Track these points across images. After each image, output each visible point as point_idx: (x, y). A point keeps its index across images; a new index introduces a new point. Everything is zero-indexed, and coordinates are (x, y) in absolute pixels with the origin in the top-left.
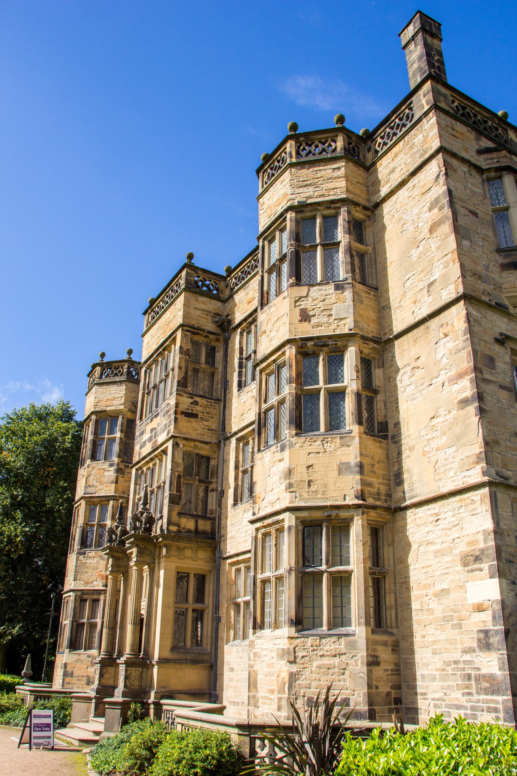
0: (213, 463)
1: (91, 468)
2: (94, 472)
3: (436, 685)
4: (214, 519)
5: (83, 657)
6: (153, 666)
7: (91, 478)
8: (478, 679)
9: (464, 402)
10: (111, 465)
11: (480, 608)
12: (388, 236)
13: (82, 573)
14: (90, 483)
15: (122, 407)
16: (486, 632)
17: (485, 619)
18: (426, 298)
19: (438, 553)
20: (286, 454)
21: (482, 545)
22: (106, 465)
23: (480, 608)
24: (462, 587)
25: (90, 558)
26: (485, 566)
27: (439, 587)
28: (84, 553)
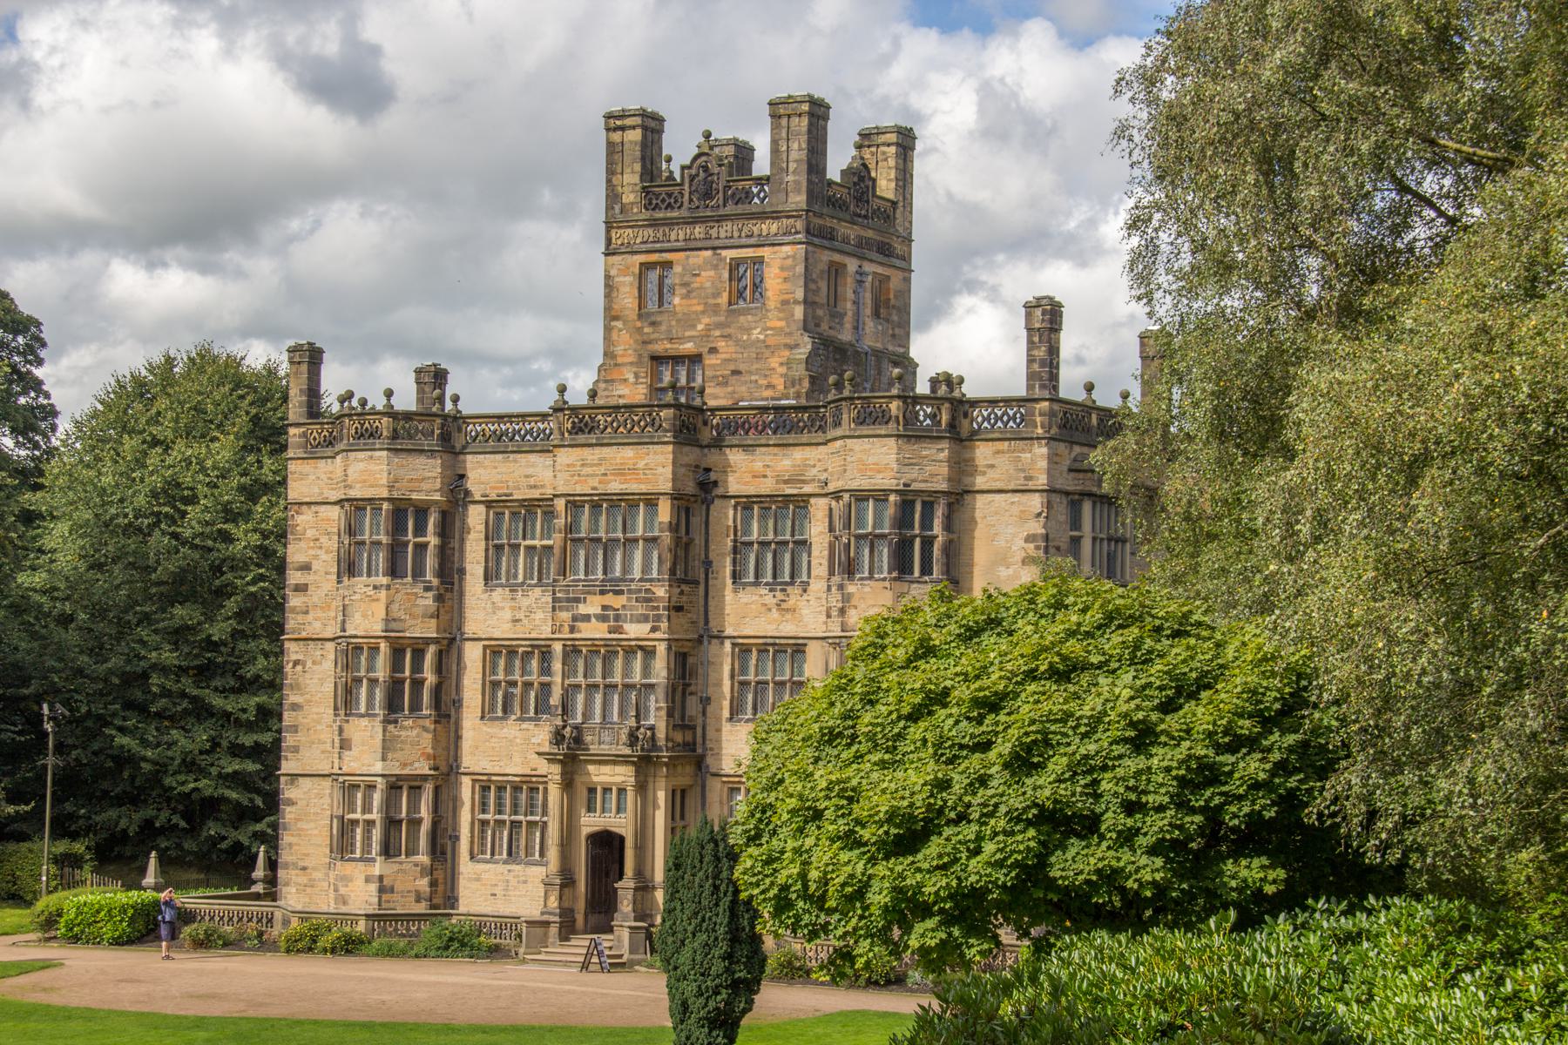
0: (690, 660)
1: (392, 591)
2: (399, 597)
4: (693, 728)
6: (654, 888)
7: (395, 607)
10: (427, 589)
12: (977, 534)
13: (395, 750)
14: (395, 615)
15: (437, 497)
22: (419, 589)
25: (405, 728)
28: (396, 722)
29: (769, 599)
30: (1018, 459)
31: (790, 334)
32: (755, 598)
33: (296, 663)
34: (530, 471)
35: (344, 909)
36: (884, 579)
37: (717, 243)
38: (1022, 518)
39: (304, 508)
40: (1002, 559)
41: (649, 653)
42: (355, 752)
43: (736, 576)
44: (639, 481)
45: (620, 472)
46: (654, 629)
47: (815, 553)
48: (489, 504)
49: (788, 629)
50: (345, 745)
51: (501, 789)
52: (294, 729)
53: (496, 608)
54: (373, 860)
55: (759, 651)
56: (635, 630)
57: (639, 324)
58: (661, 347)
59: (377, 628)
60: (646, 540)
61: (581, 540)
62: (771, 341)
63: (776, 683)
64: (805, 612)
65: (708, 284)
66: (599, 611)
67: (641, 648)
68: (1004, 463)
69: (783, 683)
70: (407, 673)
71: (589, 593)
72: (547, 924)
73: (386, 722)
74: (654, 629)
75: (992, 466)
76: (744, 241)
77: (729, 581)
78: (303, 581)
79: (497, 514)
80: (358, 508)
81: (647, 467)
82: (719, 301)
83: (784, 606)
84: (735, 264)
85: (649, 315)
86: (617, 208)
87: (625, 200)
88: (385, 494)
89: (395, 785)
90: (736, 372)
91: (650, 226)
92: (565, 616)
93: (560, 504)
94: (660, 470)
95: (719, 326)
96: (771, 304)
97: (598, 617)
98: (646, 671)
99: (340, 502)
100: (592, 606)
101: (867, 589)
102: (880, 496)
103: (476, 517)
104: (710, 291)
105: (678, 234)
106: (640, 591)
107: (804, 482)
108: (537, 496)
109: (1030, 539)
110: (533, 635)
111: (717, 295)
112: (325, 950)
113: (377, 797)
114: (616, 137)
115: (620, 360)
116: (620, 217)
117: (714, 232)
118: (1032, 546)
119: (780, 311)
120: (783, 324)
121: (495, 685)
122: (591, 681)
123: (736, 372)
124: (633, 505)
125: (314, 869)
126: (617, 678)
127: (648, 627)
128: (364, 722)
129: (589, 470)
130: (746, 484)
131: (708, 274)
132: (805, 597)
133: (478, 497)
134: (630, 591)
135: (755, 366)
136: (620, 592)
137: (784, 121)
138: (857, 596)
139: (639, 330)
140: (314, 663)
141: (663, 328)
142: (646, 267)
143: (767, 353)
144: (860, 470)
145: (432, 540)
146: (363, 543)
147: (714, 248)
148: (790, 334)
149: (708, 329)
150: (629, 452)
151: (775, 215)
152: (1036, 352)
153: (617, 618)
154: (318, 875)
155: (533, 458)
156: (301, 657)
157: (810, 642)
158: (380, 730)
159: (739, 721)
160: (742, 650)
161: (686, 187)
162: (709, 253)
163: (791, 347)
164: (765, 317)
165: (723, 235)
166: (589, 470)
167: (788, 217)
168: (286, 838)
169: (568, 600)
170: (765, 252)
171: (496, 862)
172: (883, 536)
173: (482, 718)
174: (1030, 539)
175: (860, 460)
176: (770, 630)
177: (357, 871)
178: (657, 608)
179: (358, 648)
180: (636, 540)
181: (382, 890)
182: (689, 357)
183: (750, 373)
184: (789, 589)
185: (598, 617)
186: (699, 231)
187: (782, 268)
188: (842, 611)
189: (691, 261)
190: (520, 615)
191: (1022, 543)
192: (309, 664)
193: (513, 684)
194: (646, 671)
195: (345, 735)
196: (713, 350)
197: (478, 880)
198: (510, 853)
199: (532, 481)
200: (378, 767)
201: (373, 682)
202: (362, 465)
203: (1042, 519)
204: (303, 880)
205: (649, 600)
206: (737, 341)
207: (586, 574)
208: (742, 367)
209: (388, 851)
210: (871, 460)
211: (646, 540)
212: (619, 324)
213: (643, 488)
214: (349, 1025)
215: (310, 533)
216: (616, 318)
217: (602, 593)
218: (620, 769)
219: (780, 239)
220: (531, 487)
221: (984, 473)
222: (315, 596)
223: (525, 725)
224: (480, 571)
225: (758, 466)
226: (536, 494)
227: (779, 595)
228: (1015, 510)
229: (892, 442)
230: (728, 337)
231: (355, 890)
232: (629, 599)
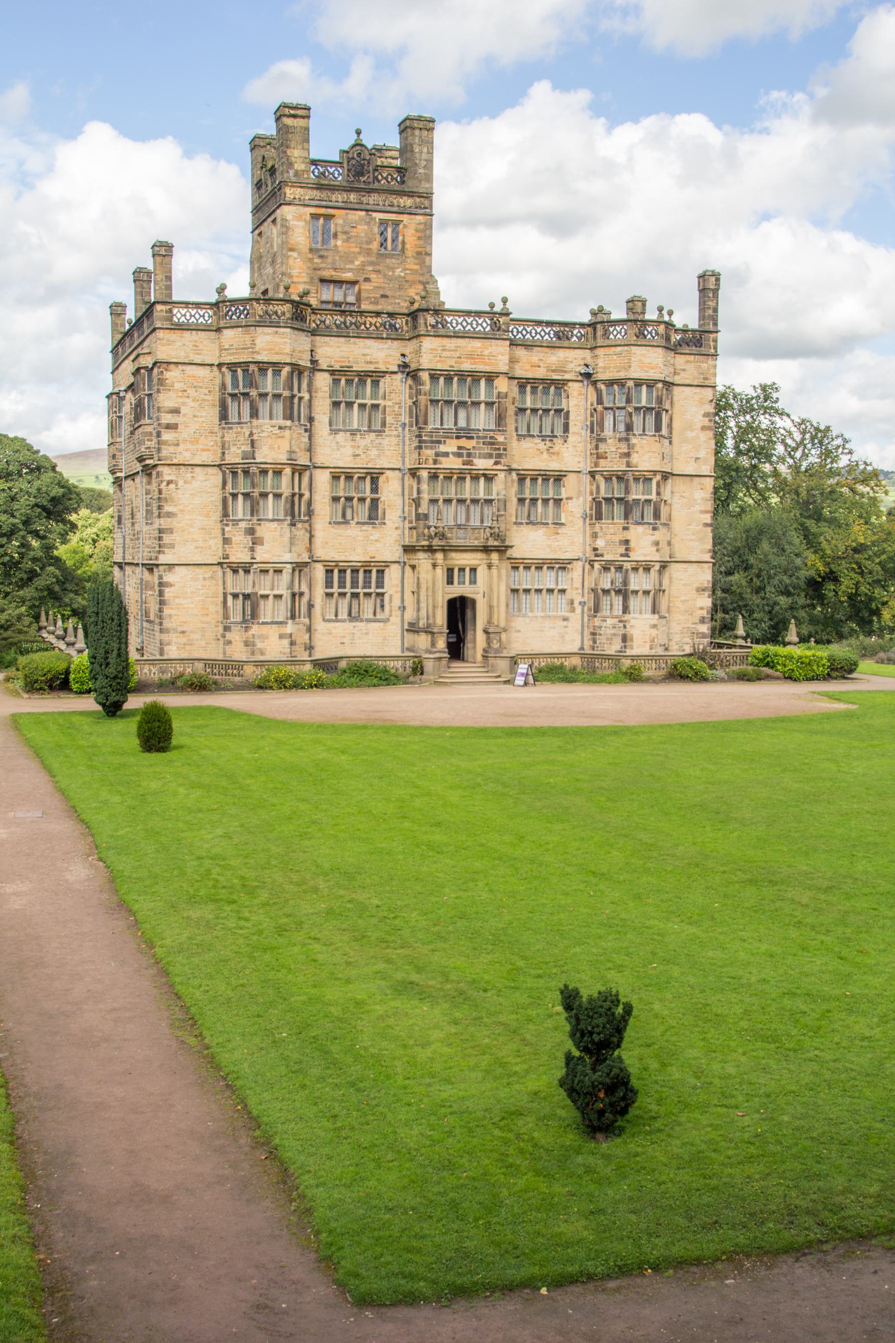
3: (678, 636)
5: (301, 626)
8: (697, 634)
9: (706, 525)
10: (306, 431)
11: (702, 608)
16: (704, 618)
17: (704, 613)
18: (693, 463)
19: (685, 585)
20: (656, 532)
21: (706, 585)
23: (702, 608)
24: (695, 600)
26: (706, 594)
27: (683, 598)
28: (294, 525)
29: (542, 446)
30: (700, 367)
31: (423, 274)
32: (532, 445)
33: (169, 483)
34: (367, 351)
35: (262, 658)
36: (655, 436)
37: (369, 207)
38: (701, 402)
39: (172, 367)
40: (690, 427)
41: (489, 479)
42: (267, 546)
43: (517, 430)
44: (485, 364)
45: (471, 357)
46: (496, 463)
47: (572, 417)
48: (332, 372)
49: (554, 465)
50: (256, 542)
51: (342, 572)
52: (170, 531)
53: (339, 446)
54: (287, 623)
55: (532, 479)
56: (482, 464)
57: (310, 256)
58: (327, 274)
59: (283, 458)
60: (487, 404)
61: (438, 401)
62: (409, 278)
63: (543, 500)
64: (565, 455)
65: (363, 235)
66: (455, 450)
67: (484, 475)
68: (690, 368)
69: (548, 500)
70: (297, 490)
71: (448, 437)
72: (440, 658)
73: (293, 524)
74: (496, 463)
75: (684, 370)
76: (389, 209)
77: (515, 434)
78: (173, 422)
79: (333, 379)
80: (260, 369)
81: (491, 355)
82: (371, 247)
83: (551, 450)
84: (383, 222)
85: (318, 250)
86: (292, 172)
87: (296, 166)
88: (288, 361)
89: (299, 567)
90: (384, 296)
91: (317, 189)
92: (429, 453)
93: (425, 376)
94: (500, 357)
95: (371, 263)
96: (410, 251)
97: (454, 454)
98: (488, 491)
99: (232, 367)
100: (451, 446)
101: (644, 441)
102: (651, 384)
103: (323, 381)
104: (364, 239)
105: (338, 197)
106: (486, 437)
107: (565, 372)
108: (373, 369)
109: (706, 415)
110: (369, 466)
111: (369, 242)
112: (312, 687)
113: (286, 576)
114: (289, 121)
115: (295, 280)
116: (294, 179)
117: (364, 200)
118: (707, 419)
119: (415, 258)
120: (418, 267)
121: (336, 499)
122: (447, 497)
123: (384, 296)
124: (476, 380)
125: (192, 632)
126: (467, 495)
127: (492, 461)
128: (274, 525)
129: (447, 354)
130: (526, 370)
131: (362, 228)
132: (566, 445)
133: (325, 368)
134: (478, 438)
135: (398, 294)
136: (472, 438)
137: (417, 132)
138: (638, 446)
139: (311, 260)
140: (186, 482)
141: (329, 260)
142: (315, 217)
143: (407, 286)
144: (640, 367)
145: (307, 396)
146: (266, 395)
147: (367, 211)
148: (423, 274)
149: (363, 264)
151: (411, 194)
152: (710, 303)
153: (469, 455)
154: (193, 636)
155: (369, 342)
156: (173, 478)
157: (571, 475)
158: (288, 531)
159: (522, 524)
160: (522, 479)
161: (345, 165)
162: (363, 213)
163: (424, 284)
164: (404, 261)
165: (371, 202)
166: (447, 354)
167: (419, 197)
168: (167, 611)
169: (432, 442)
170: (405, 218)
171: (343, 621)
172: (653, 409)
173: (330, 523)
174: (706, 415)
175: (640, 360)
177: (273, 632)
178: (499, 449)
179: (264, 472)
180: (479, 403)
181: (292, 643)
182: (347, 282)
183: (394, 297)
184: (555, 440)
185: (454, 454)
186: (353, 197)
187: (417, 231)
188: (628, 455)
189: (350, 217)
190: (360, 452)
191: (701, 417)
192: (181, 483)
193: (349, 499)
194: (488, 491)
195: (258, 534)
196: (367, 280)
197: (330, 633)
198: (350, 614)
199: (368, 358)
200: (287, 557)
201: (278, 496)
202: (268, 338)
203: (713, 404)
204: (183, 640)
205: (493, 444)
206: (385, 276)
207: (442, 424)
208: (388, 293)
209: (293, 617)
210: (647, 361)
211: (487, 404)
212: (295, 254)
213: (488, 369)
214: (482, 732)
215: (178, 386)
216: (292, 250)
217: (458, 438)
218: (479, 555)
219: (414, 211)
220: (368, 363)
221: (679, 374)
222: (184, 433)
223: (365, 527)
224: (326, 420)
225: (535, 359)
227: (549, 444)
228: (697, 397)
229: (660, 350)
230: (378, 272)
231: (273, 645)
232: (478, 443)
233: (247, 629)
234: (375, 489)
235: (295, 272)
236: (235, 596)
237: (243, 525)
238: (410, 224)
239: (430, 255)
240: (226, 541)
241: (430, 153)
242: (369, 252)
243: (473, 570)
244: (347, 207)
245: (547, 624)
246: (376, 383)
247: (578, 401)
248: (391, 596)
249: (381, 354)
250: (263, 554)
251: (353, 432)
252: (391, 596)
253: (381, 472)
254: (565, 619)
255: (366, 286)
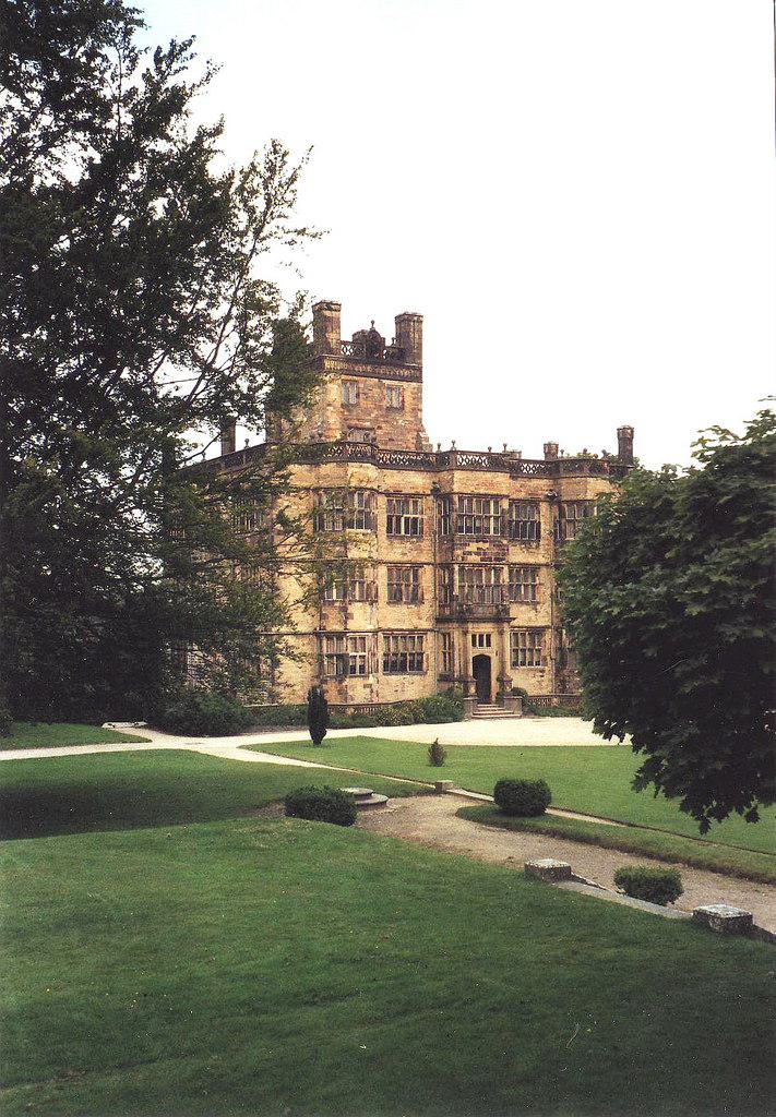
47: (542, 526)
49: (532, 560)
50: (348, 617)
58: (353, 423)
92: (459, 552)
93: (456, 498)
98: (497, 577)
100: (473, 547)
111: (380, 401)
115: (332, 427)
131: (376, 390)
147: (379, 378)
150: (489, 475)
153: (485, 554)
170: (405, 384)
176: (524, 561)
195: (349, 611)
196: (380, 428)
200: (370, 627)
212: (331, 408)
213: (495, 493)
216: (329, 405)
226: (413, 491)
233: (341, 682)
234: (416, 578)
235: (331, 421)
236: (330, 656)
237: (337, 604)
238: (409, 387)
239: (421, 410)
240: (323, 617)
241: (420, 338)
242: (380, 408)
243: (489, 636)
244: (365, 375)
245: (531, 674)
246: (415, 503)
247: (545, 517)
248: (428, 655)
249: (417, 481)
250: (352, 625)
251: (402, 538)
252: (428, 655)
253: (421, 565)
254: (543, 671)
255: (379, 432)
